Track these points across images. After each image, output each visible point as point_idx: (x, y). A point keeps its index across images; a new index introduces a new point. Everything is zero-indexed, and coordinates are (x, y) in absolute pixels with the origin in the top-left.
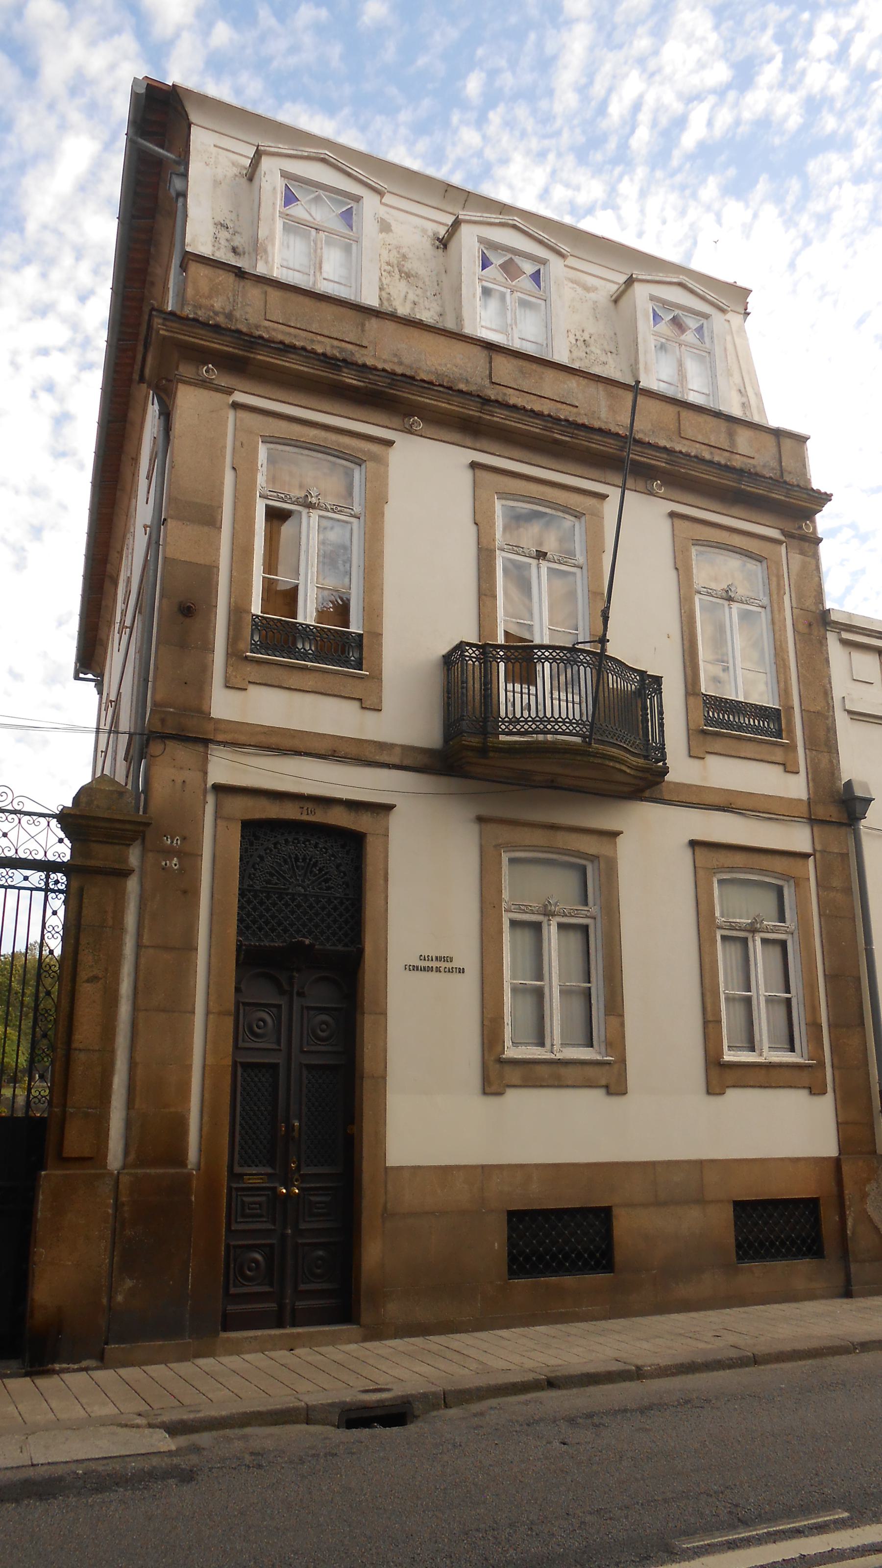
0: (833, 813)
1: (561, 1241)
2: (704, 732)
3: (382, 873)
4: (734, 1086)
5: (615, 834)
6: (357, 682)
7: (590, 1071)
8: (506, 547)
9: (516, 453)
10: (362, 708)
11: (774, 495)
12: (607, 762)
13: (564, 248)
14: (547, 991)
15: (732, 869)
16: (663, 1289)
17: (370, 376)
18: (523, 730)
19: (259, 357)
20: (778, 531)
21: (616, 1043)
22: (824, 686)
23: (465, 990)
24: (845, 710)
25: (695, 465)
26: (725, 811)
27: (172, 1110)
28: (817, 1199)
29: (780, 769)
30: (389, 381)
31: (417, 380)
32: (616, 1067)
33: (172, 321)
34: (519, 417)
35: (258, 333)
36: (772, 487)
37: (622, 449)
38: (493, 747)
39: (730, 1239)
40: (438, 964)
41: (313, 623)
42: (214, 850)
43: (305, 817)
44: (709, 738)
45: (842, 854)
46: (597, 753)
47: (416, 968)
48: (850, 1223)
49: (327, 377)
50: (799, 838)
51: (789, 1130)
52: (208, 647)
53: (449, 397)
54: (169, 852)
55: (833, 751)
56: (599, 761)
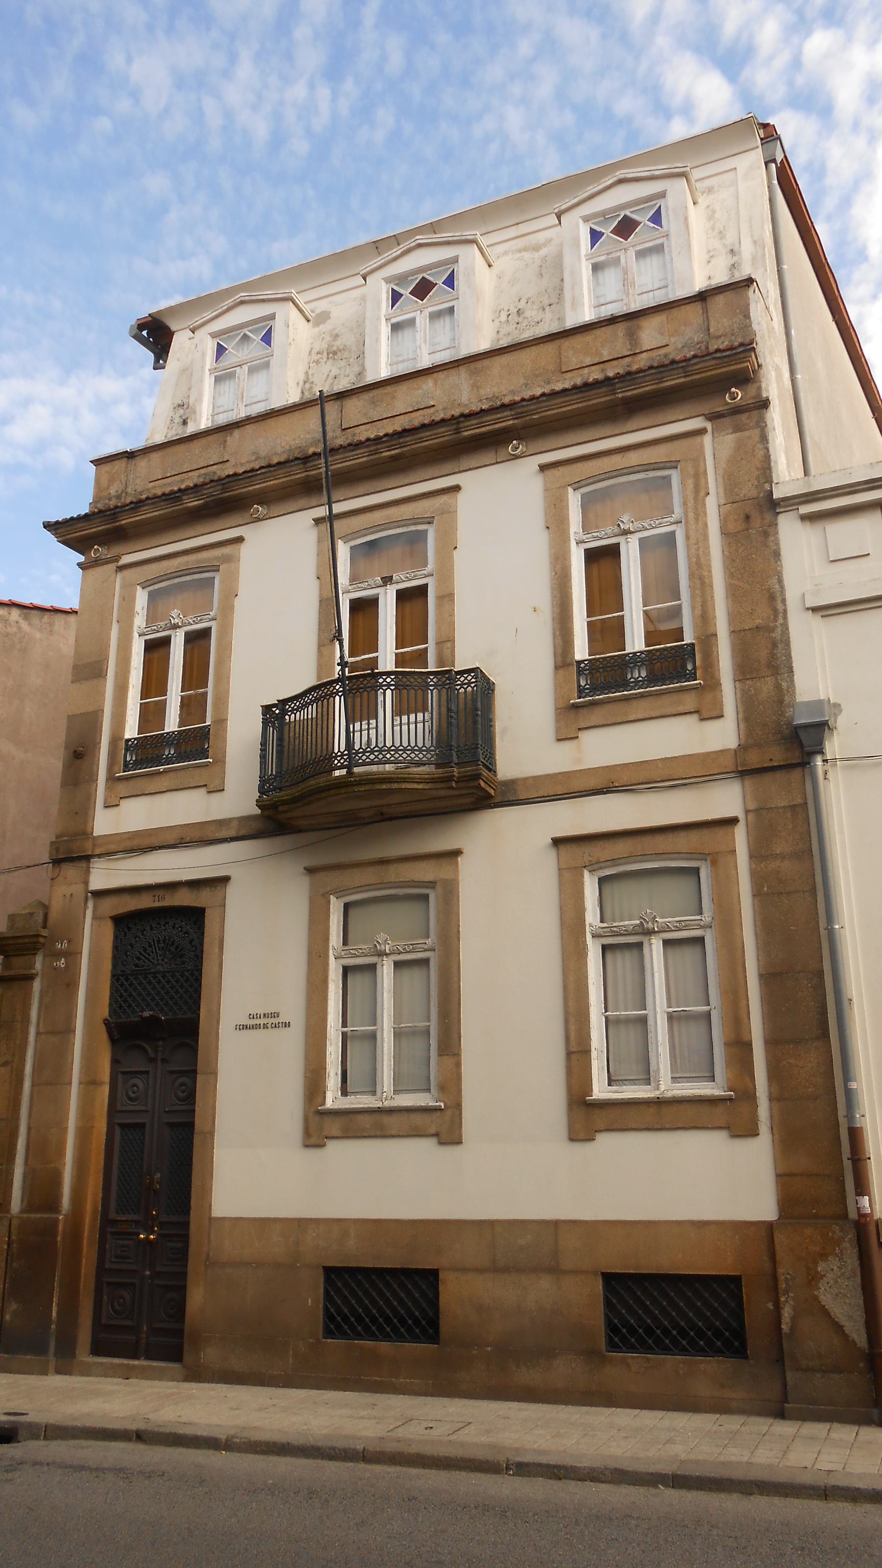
0: (776, 755)
1: (383, 1305)
2: (575, 706)
3: (217, 942)
4: (607, 1130)
5: (457, 853)
6: (203, 770)
7: (418, 1119)
8: (350, 588)
9: (361, 489)
10: (209, 792)
11: (668, 384)
12: (378, 787)
13: (468, 234)
14: (650, 1021)
15: (614, 862)
16: (504, 1368)
17: (205, 492)
18: (417, 759)
19: (123, 522)
20: (700, 418)
21: (451, 1087)
22: (769, 590)
23: (290, 1045)
24: (808, 609)
25: (548, 403)
26: (605, 793)
27: (53, 1165)
28: (736, 1280)
29: (693, 719)
30: (220, 487)
31: (240, 475)
32: (449, 1112)
33: (61, 528)
34: (342, 456)
35: (144, 497)
36: (659, 376)
37: (458, 431)
38: (278, 801)
39: (596, 1320)
40: (265, 1021)
41: (588, 657)
42: (92, 944)
43: (157, 904)
44: (584, 711)
45: (793, 808)
46: (360, 780)
47: (245, 1027)
48: (787, 1313)
49: (174, 511)
50: (726, 800)
51: (713, 1184)
52: (93, 778)
53: (274, 473)
54: (58, 955)
55: (784, 670)
56: (367, 787)
